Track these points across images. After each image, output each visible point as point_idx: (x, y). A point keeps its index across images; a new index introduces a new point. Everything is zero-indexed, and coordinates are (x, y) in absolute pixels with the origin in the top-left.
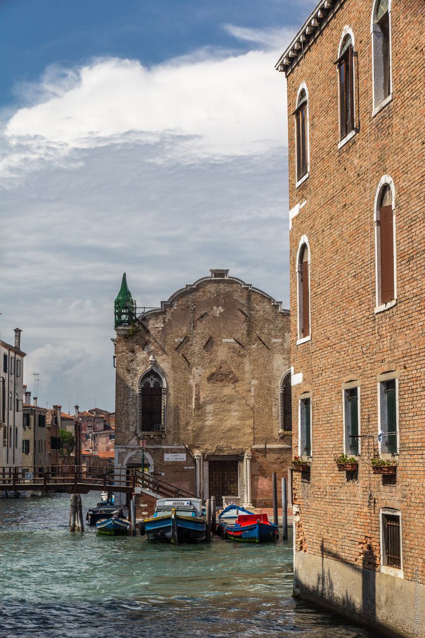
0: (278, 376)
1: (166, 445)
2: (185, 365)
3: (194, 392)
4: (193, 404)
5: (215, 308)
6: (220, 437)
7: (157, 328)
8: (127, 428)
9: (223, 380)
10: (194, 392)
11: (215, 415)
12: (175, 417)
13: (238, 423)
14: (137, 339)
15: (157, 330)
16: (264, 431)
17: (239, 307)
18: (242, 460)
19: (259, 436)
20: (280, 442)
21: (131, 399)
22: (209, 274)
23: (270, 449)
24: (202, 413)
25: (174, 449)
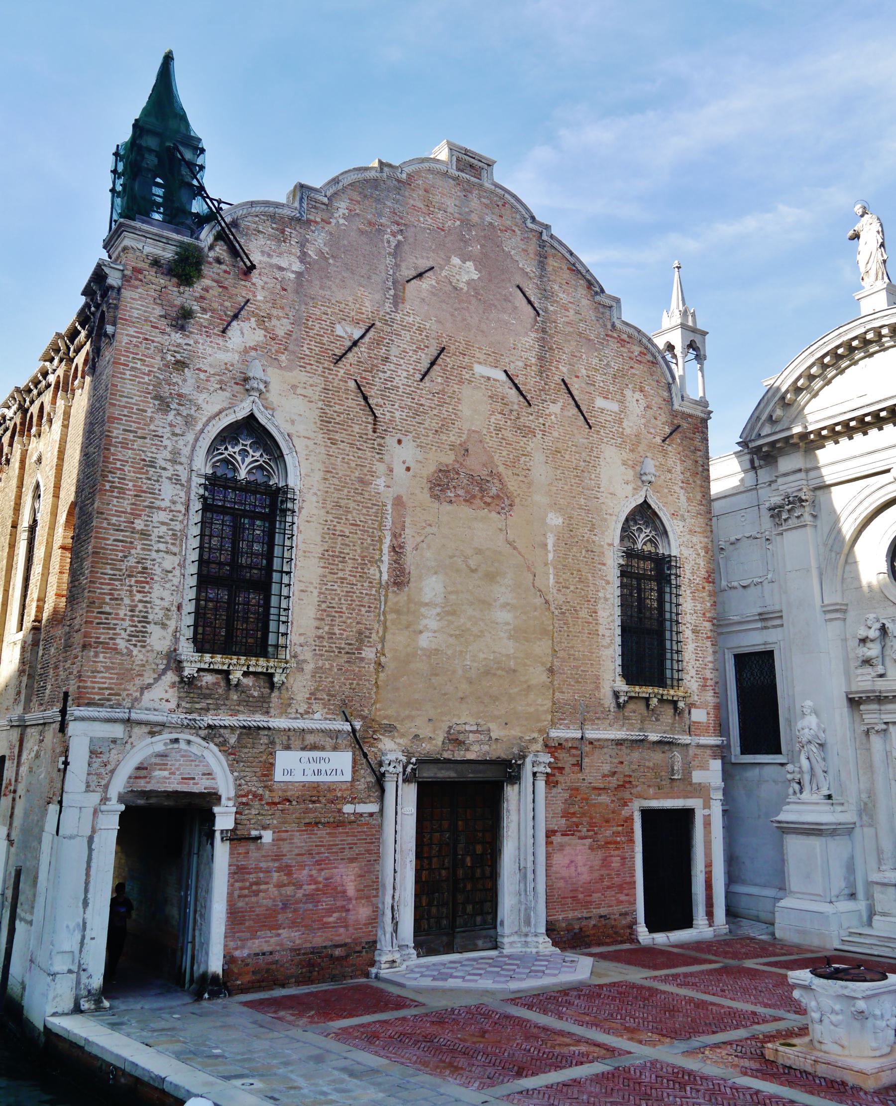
0: (610, 511)
1: (285, 708)
2: (361, 424)
3: (389, 523)
4: (385, 568)
5: (456, 261)
6: (460, 694)
7: (281, 269)
8: (139, 636)
9: (474, 497)
10: (389, 523)
11: (448, 613)
12: (324, 606)
13: (508, 647)
14: (206, 290)
15: (279, 275)
16: (577, 682)
17: (519, 279)
18: (515, 779)
19: (566, 696)
20: (616, 719)
21: (163, 516)
22: (443, 154)
23: (591, 743)
24: (410, 600)
25: (311, 731)
